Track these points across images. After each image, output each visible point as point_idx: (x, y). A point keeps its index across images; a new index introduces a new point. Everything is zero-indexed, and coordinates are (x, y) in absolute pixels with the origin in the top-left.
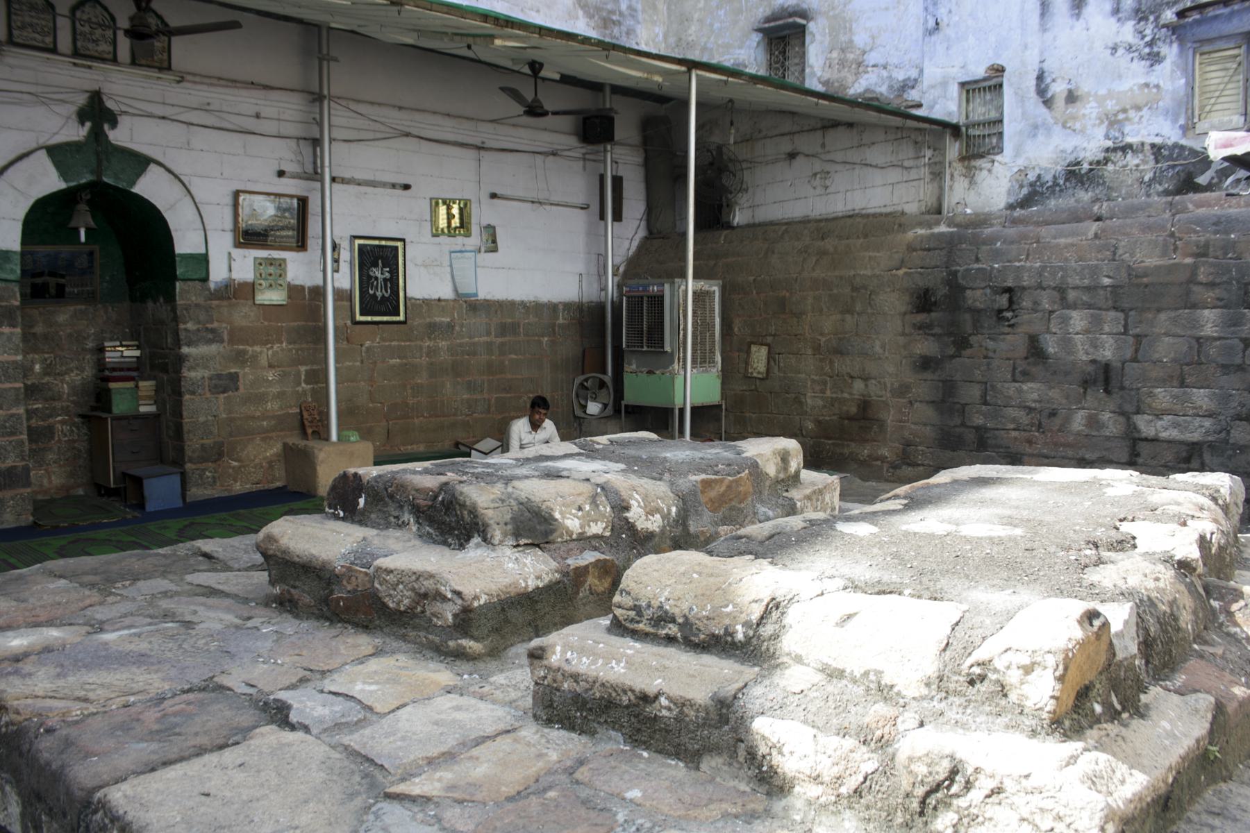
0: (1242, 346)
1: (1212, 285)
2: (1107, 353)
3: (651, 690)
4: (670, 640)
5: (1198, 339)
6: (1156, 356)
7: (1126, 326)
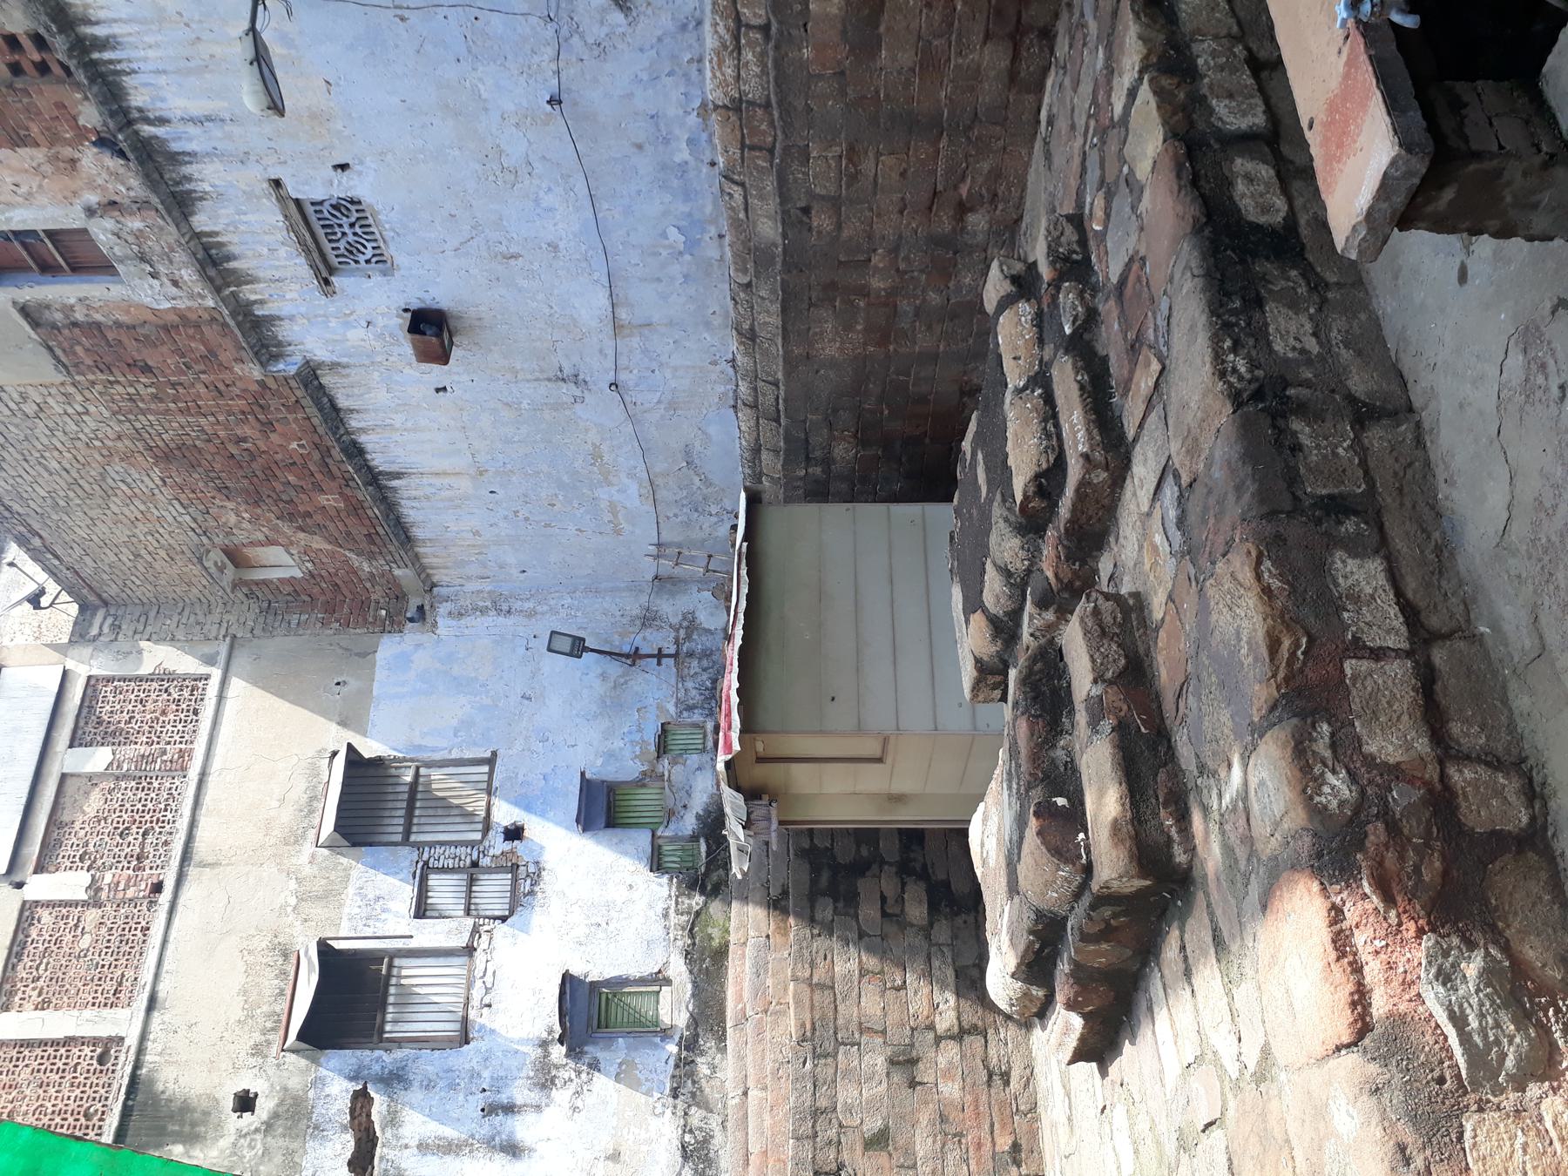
1: (812, 965)
2: (880, 1061)
3: (1075, 387)
4: (1057, 426)
5: (861, 975)
6: (879, 1013)
7: (853, 1045)
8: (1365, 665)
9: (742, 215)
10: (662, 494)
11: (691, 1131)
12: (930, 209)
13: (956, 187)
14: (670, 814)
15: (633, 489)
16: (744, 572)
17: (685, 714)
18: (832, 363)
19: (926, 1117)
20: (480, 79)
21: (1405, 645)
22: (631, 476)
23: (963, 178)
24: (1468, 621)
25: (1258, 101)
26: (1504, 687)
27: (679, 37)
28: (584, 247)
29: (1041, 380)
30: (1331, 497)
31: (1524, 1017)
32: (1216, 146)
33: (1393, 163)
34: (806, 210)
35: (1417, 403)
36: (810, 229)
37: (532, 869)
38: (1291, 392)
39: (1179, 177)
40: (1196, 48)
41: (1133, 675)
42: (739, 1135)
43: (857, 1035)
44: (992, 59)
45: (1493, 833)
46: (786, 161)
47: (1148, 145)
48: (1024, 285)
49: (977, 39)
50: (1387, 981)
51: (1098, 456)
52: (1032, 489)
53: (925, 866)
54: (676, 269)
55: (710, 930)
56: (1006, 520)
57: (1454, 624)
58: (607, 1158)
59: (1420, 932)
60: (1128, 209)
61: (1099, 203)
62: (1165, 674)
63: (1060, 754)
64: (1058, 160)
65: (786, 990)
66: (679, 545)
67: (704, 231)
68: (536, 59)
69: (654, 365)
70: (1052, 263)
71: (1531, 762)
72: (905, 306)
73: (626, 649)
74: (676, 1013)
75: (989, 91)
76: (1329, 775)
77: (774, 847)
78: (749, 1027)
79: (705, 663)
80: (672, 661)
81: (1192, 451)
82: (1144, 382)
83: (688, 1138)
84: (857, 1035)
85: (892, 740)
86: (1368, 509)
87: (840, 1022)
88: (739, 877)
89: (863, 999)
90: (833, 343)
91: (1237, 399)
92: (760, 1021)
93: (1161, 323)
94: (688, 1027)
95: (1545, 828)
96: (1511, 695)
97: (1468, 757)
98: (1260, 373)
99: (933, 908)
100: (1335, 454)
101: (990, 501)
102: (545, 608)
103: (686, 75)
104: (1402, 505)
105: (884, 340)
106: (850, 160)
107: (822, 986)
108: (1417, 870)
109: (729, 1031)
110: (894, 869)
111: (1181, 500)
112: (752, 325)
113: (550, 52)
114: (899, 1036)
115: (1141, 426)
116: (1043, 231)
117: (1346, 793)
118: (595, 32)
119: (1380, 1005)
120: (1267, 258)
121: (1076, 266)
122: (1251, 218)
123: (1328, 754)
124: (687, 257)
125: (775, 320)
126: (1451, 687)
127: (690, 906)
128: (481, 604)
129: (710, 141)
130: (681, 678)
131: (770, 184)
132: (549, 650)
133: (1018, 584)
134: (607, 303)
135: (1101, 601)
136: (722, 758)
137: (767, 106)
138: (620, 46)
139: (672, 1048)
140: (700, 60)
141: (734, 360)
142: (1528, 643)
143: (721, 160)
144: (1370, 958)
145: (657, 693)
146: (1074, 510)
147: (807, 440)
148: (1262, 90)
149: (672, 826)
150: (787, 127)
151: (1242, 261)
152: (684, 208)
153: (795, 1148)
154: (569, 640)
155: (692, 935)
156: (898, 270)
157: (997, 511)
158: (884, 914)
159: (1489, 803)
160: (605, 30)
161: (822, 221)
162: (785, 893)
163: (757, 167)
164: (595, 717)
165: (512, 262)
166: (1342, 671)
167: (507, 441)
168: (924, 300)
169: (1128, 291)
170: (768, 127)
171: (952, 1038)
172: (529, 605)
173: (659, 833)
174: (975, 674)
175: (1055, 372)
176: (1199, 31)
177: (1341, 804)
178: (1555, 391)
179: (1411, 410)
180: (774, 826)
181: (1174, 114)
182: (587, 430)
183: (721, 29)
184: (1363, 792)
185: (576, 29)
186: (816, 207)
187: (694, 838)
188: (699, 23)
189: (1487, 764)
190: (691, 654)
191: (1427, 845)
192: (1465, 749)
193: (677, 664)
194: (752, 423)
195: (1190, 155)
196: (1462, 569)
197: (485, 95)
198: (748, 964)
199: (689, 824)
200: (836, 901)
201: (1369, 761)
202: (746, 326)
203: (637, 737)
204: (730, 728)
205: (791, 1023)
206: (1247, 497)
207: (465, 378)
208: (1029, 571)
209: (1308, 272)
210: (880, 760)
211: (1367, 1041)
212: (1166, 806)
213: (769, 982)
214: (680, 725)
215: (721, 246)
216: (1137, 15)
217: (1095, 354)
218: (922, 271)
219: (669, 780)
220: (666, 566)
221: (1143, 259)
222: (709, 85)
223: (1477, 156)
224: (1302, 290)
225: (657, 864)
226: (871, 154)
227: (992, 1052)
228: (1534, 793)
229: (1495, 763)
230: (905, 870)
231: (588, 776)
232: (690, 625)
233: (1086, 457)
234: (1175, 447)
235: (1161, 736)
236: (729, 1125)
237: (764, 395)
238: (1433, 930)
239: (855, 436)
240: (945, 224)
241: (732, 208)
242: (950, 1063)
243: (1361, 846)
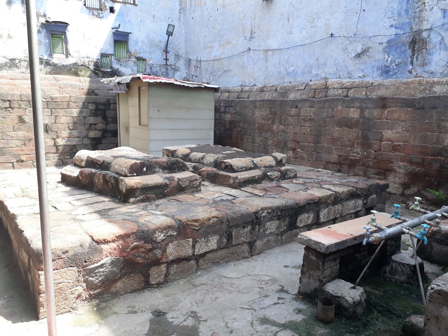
0: (83, 119)
1: (75, 102)
3: (254, 175)
4: (244, 171)
5: (72, 117)
6: (61, 122)
7: (51, 113)
8: (191, 244)
9: (296, 89)
10: (216, 63)
11: (20, 62)
12: (294, 141)
13: (300, 148)
14: (119, 60)
15: (218, 54)
16: (195, 86)
17: (149, 67)
18: (253, 114)
19: (30, 135)
20: (340, 13)
21: (195, 254)
22: (222, 53)
23: (302, 150)
24: (201, 269)
25: (326, 220)
26: (185, 278)
27: (347, 72)
28: (290, 42)
29: (256, 167)
30: (232, 236)
31: (103, 282)
32: (316, 209)
33: (323, 244)
34: (297, 107)
35: (254, 257)
36: (291, 108)
37: (101, 15)
38: (257, 226)
39: (310, 200)
40: (340, 205)
41: (180, 189)
42: (20, 77)
43: (54, 115)
44: (334, 157)
45: (149, 275)
46: (310, 102)
47: (317, 193)
48: (279, 163)
49: (339, 153)
50: (111, 249)
51: (237, 181)
52: (227, 164)
53: (106, 137)
54: (282, 69)
55: (83, 71)
56: (218, 158)
57: (200, 266)
58: (9, 34)
59: (124, 257)
60: (300, 188)
61: (301, 182)
62: (181, 197)
63: (157, 169)
64: (309, 173)
65: (67, 94)
66: (200, 67)
67: (292, 77)
68: (344, 30)
69: (255, 62)
70: (285, 170)
71: (167, 284)
72: (269, 134)
73: (168, 49)
74: (58, 59)
75: (325, 157)
76: (163, 234)
77: (111, 92)
78: (54, 82)
79: (164, 73)
80: (165, 63)
81: (241, 203)
82: (256, 192)
83: (17, 61)
84: (54, 115)
85: (146, 128)
86: (229, 245)
87: (58, 110)
88: (102, 81)
89: (65, 117)
90: (259, 114)
91: (256, 213)
92: (57, 85)
93: (272, 196)
94: (53, 63)
95: (150, 288)
96: (183, 280)
97: (168, 269)
98: (262, 219)
99: (93, 139)
100: (242, 237)
101: (223, 154)
102: (181, 24)
104: (229, 253)
105: (259, 129)
106: (309, 119)
107: (68, 105)
108: (140, 256)
109: (53, 76)
110: (105, 128)
111: (228, 200)
112: (265, 91)
113: (346, 35)
114: (54, 127)
115: (245, 191)
116: (293, 168)
117: (159, 238)
118: (350, 48)
119: (104, 247)
120: (289, 221)
121: (284, 176)
122: (299, 218)
123: (169, 234)
124: (285, 73)
125: (266, 98)
126: (185, 265)
127: (91, 65)
128: (183, 4)
129: (317, 80)
130: (160, 66)
131: (304, 97)
132: (169, 25)
133: (200, 161)
134: (274, 48)
135: (199, 181)
136: (141, 76)
137: (326, 96)
138: (345, 55)
139: (46, 57)
140: (339, 78)
141: (255, 85)
142: (197, 283)
143: (312, 83)
144: (117, 244)
145: (155, 58)
146: (222, 175)
147: (232, 106)
148: (328, 221)
149: (115, 61)
150: (320, 102)
151: (289, 215)
152: (299, 72)
153: (18, 95)
154: (172, 31)
155: (82, 65)
156: (278, 132)
157: (221, 156)
158: (91, 124)
159: (156, 274)
160: (350, 51)
161: (293, 111)
162: (96, 95)
163: (309, 94)
164: (148, 38)
165: (287, 20)
166: (189, 238)
167: (234, 16)
168: (269, 140)
169: (279, 188)
170: (320, 96)
171: (55, 143)
172: (182, 20)
173: (113, 56)
174: (172, 150)
175: (258, 170)
176: (344, 206)
177: (156, 238)
178: (261, 286)
179: (252, 256)
180: (118, 92)
181: (325, 199)
182: (236, 40)
183: (348, 84)
184: (159, 243)
186: (297, 110)
187: (111, 68)
188: (350, 78)
189: (166, 273)
190: (167, 69)
191: (146, 259)
192: (170, 268)
193: (164, 65)
194: (237, 91)
195: (315, 203)
196: (213, 268)
198: (74, 83)
199: (116, 66)
200: (95, 110)
201: (167, 245)
202: (265, 89)
203: (142, 51)
204: (150, 79)
205: (56, 95)
206: (232, 215)
207: (253, 4)
208: (203, 164)
209: (285, 231)
210: (140, 124)
211: (95, 243)
212: (146, 196)
213: (69, 89)
214: (146, 64)
215: (288, 83)
216: (349, 191)
217: (262, 180)
218: (277, 139)
219: (129, 60)
220: (194, 63)
221: (288, 192)
222: (333, 80)
223: (323, 264)
224: (281, 230)
225: (103, 55)
226: (311, 125)
227: (51, 155)
228: (159, 285)
229: (166, 276)
230: (104, 132)
231: (130, 35)
232: (176, 70)
233: (237, 178)
234: (242, 199)
235: (164, 196)
236: (23, 74)
237: (245, 94)
238: (124, 260)
239: (232, 121)
240: (290, 145)
241: (298, 86)
242: (47, 142)
243: (146, 242)
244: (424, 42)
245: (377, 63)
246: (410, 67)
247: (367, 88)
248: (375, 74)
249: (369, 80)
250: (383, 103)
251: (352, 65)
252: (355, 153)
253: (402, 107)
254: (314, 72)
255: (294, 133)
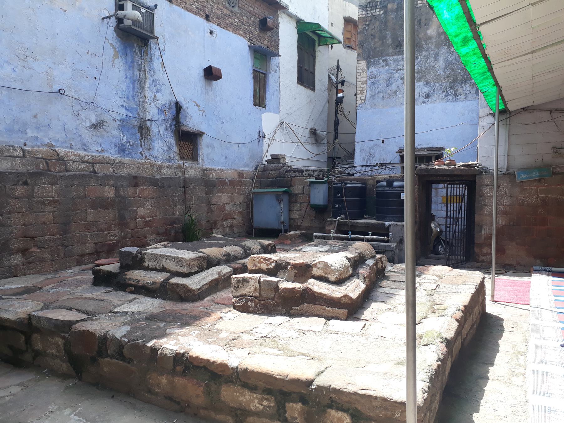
9: (6, 154)
13: (34, 246)
23: (39, 248)
44: (89, 247)
68: (73, 91)
75: (77, 249)
103: (66, 142)
106: (51, 201)
118: (83, 115)
140: (71, 148)
160: (84, 119)
161: (20, 190)
185: (83, 109)
186: (29, 188)
188: (85, 150)
197: (61, 66)
226: (53, 209)
240: (14, 246)
244: (149, 130)
245: (114, 139)
246: (141, 150)
247: (112, 164)
248: (113, 151)
249: (107, 155)
250: (135, 181)
251: (87, 136)
252: (112, 235)
253: (150, 185)
254: (30, 133)
255: (24, 225)
